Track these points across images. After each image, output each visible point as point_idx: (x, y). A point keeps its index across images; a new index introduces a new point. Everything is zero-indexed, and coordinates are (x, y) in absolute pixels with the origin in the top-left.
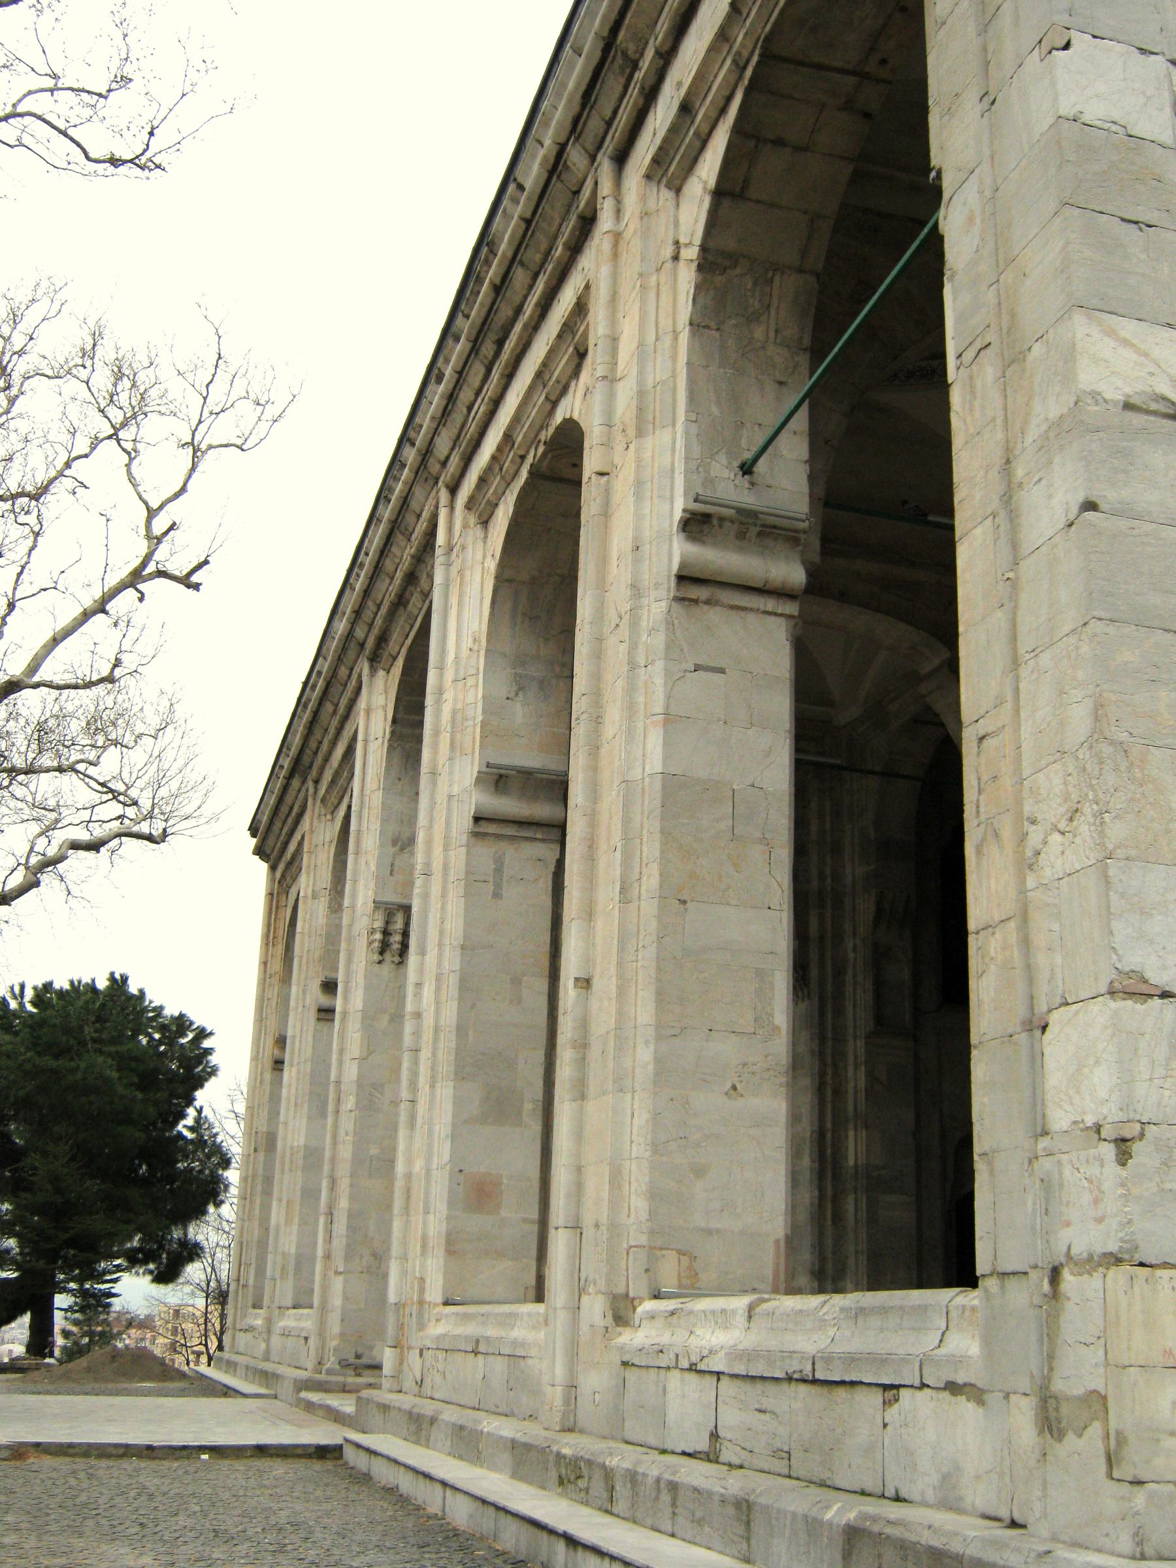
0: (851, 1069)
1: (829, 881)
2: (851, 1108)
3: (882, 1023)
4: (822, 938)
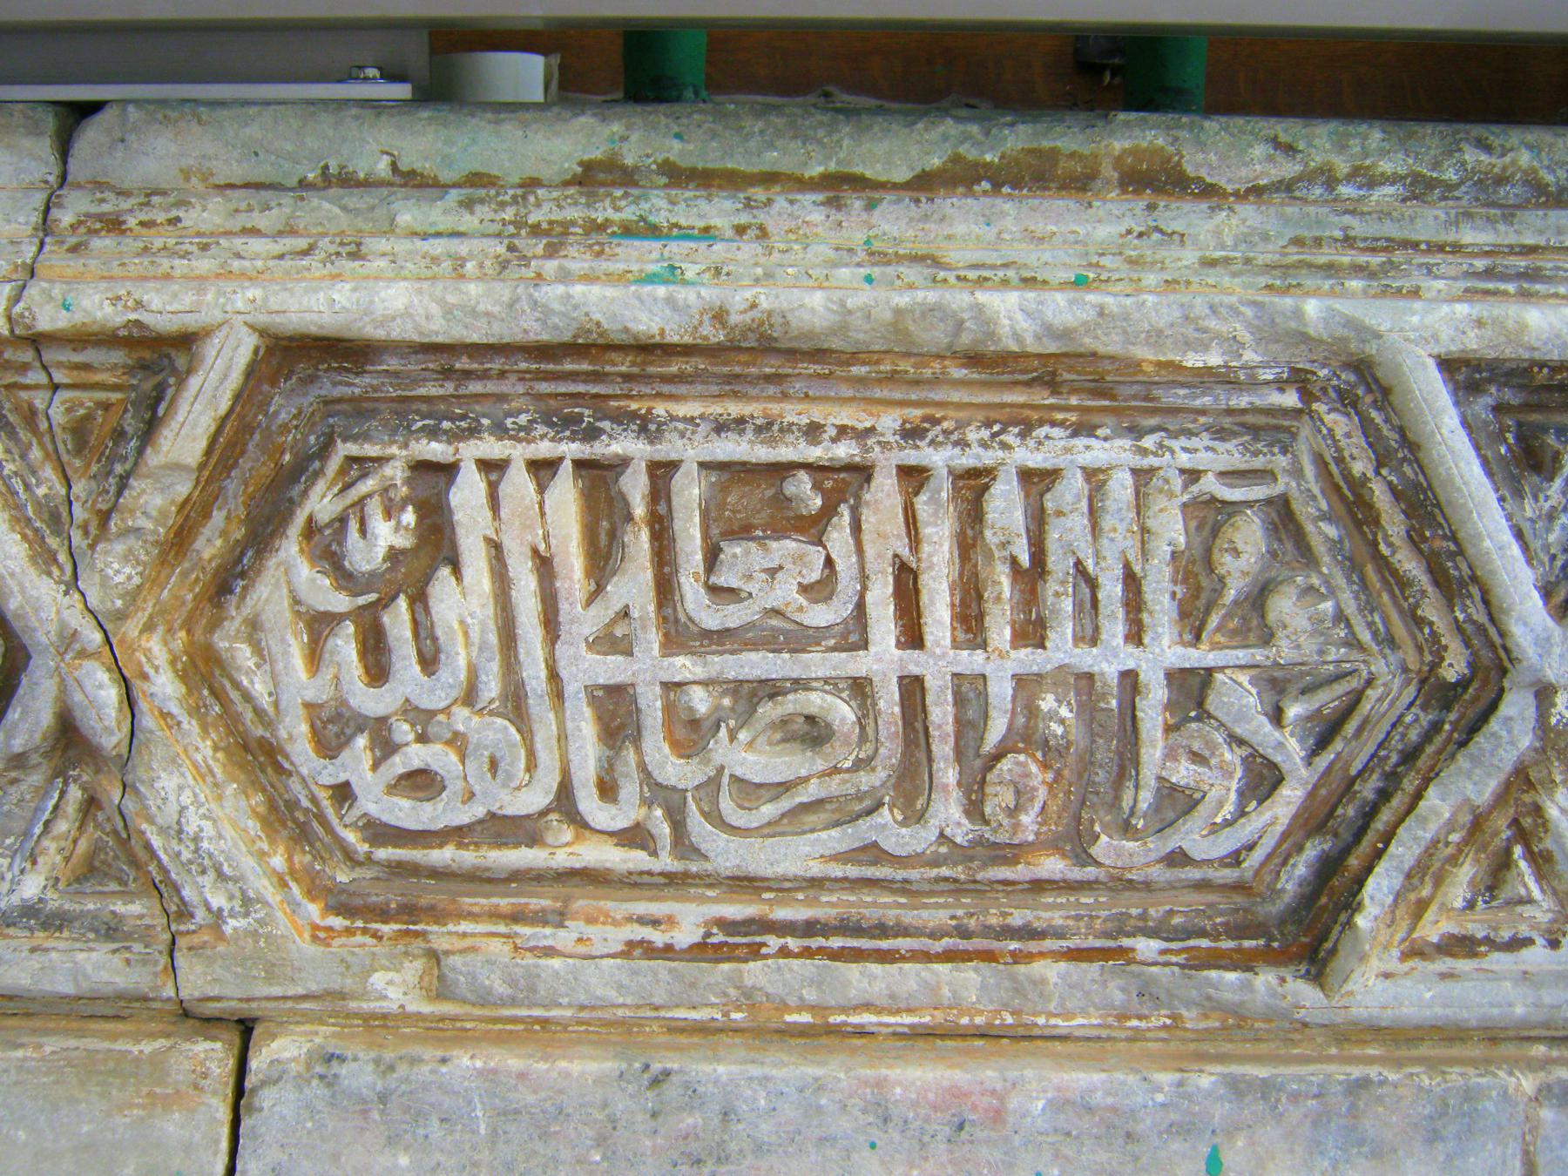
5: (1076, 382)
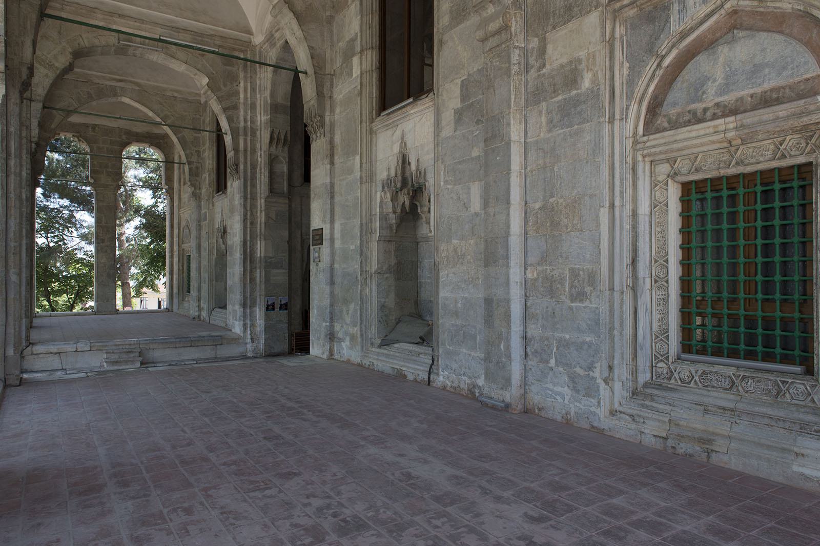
0: (259, 212)
1: (249, 123)
2: (258, 231)
3: (272, 190)
4: (245, 151)
5: (769, 380)
